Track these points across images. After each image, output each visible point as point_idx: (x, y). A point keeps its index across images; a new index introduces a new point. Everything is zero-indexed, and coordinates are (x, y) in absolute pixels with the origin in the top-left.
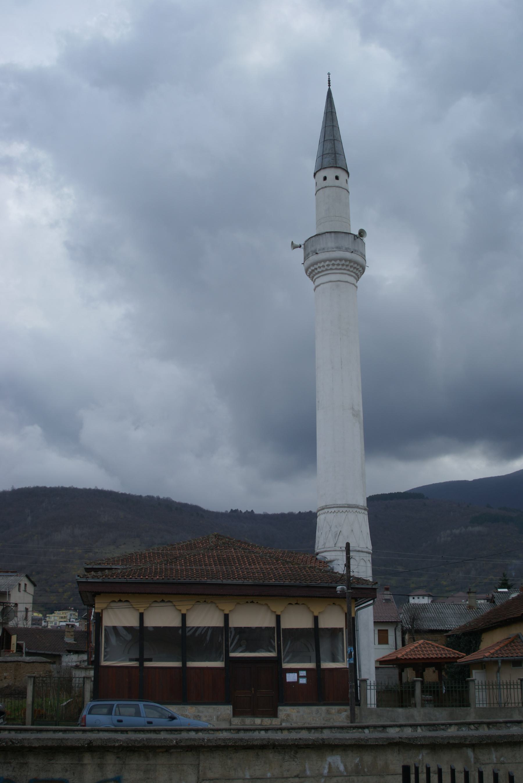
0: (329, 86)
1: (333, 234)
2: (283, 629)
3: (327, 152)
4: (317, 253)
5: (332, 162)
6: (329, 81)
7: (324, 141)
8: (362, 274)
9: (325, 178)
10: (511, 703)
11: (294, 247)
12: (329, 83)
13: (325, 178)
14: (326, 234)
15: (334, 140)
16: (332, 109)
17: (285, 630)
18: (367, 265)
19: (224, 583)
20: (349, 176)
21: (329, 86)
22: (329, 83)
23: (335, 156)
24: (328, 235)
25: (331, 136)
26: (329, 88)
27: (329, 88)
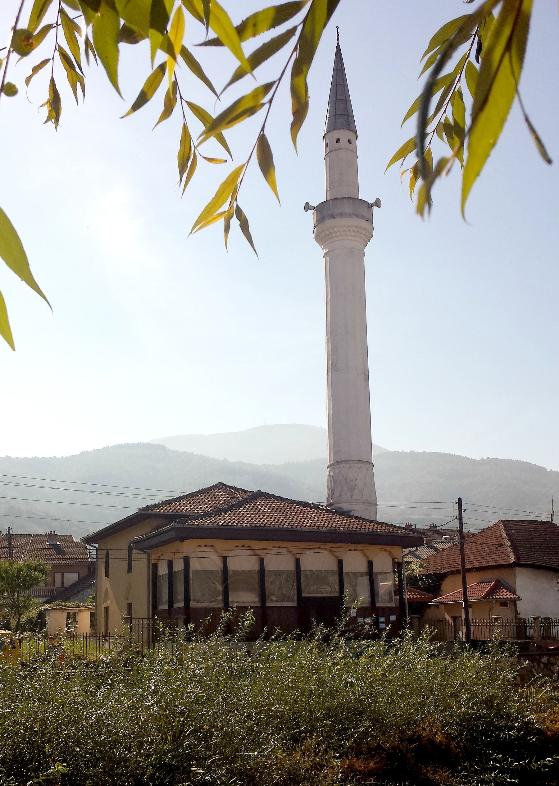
0: (338, 40)
1: (350, 201)
2: (192, 570)
3: (340, 113)
4: (334, 218)
5: (345, 124)
6: (338, 35)
7: (336, 100)
8: (369, 238)
9: (338, 140)
10: (449, 638)
11: (307, 207)
12: (338, 38)
13: (338, 140)
14: (344, 199)
15: (346, 101)
16: (342, 67)
17: (197, 572)
18: (197, 149)
19: (221, 528)
20: (196, 47)
21: (338, 40)
22: (338, 38)
23: (348, 118)
24: (345, 200)
25: (343, 96)
26: (338, 42)
27: (338, 42)
